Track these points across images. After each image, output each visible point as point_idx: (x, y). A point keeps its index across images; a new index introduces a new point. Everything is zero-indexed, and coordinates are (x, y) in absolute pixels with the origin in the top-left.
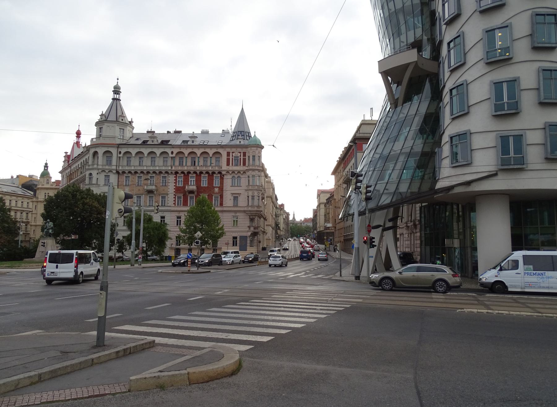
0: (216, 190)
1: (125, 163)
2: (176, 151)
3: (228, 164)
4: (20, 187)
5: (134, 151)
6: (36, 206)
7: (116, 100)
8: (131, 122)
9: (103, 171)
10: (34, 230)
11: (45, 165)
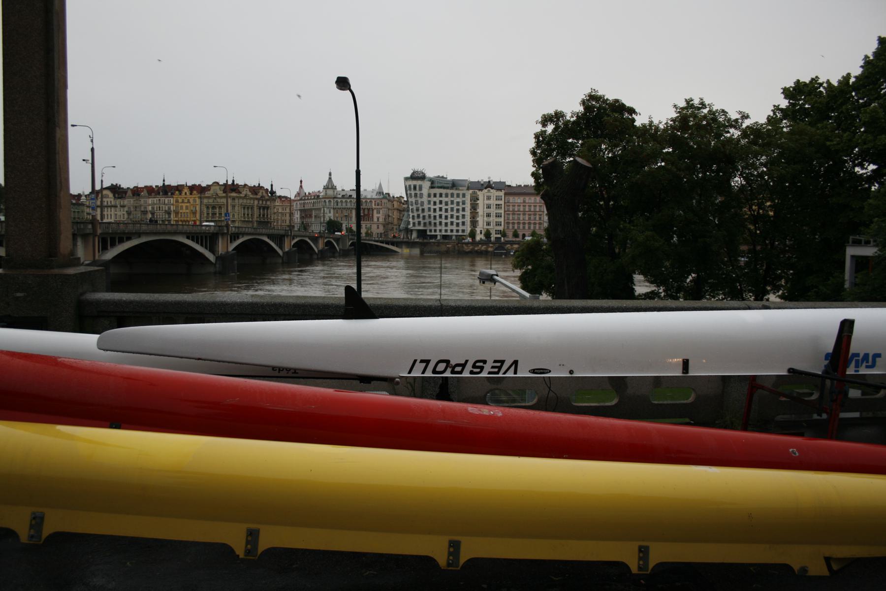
0: (371, 215)
1: (336, 204)
3: (375, 205)
5: (339, 200)
7: (330, 178)
8: (336, 187)
9: (329, 208)
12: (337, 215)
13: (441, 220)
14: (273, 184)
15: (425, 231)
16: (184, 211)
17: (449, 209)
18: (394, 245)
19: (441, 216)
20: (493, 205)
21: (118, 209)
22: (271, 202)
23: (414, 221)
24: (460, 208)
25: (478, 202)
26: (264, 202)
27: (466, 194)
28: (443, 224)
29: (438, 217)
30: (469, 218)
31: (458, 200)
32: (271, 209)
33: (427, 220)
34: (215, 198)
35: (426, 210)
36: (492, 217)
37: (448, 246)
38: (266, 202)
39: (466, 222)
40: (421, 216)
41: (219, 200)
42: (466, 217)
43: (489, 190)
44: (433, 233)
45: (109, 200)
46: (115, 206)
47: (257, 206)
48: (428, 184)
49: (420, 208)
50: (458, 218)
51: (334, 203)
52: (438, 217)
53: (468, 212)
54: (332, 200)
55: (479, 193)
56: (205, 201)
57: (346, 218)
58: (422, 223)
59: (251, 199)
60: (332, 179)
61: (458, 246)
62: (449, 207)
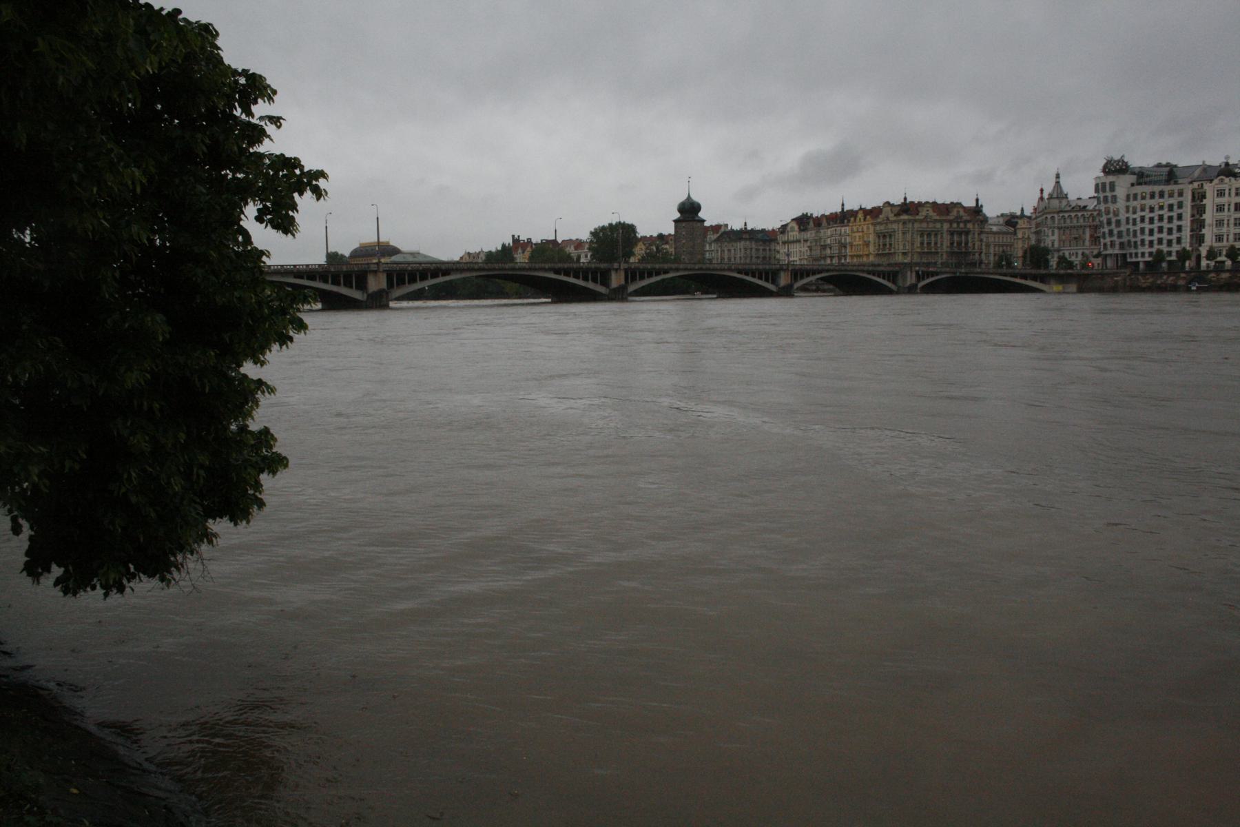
1: (1062, 221)
2: (1089, 213)
5: (1066, 215)
7: (1058, 183)
8: (1066, 195)
9: (1051, 228)
12: (1064, 237)
13: (1143, 237)
15: (1124, 256)
16: (857, 243)
17: (1156, 218)
18: (1036, 281)
19: (1142, 230)
20: (1229, 205)
21: (802, 245)
22: (974, 224)
23: (1106, 241)
24: (1174, 214)
25: (1205, 201)
26: (962, 225)
27: (1185, 191)
28: (1147, 243)
29: (1139, 232)
30: (1189, 229)
31: (1172, 201)
32: (974, 234)
33: (1125, 239)
34: (886, 223)
35: (1123, 221)
36: (1225, 226)
37: (1116, 279)
38: (965, 225)
39: (1184, 237)
40: (1115, 232)
41: (890, 226)
42: (1183, 229)
43: (1222, 179)
44: (1134, 260)
45: (794, 233)
46: (799, 241)
47: (947, 231)
48: (1133, 179)
49: (1114, 220)
50: (1170, 231)
51: (1059, 220)
52: (1139, 232)
53: (1187, 220)
54: (1056, 216)
55: (1208, 187)
56: (878, 228)
57: (1077, 241)
58: (1117, 243)
59: (936, 221)
60: (1061, 183)
61: (1131, 279)
62: (1155, 215)
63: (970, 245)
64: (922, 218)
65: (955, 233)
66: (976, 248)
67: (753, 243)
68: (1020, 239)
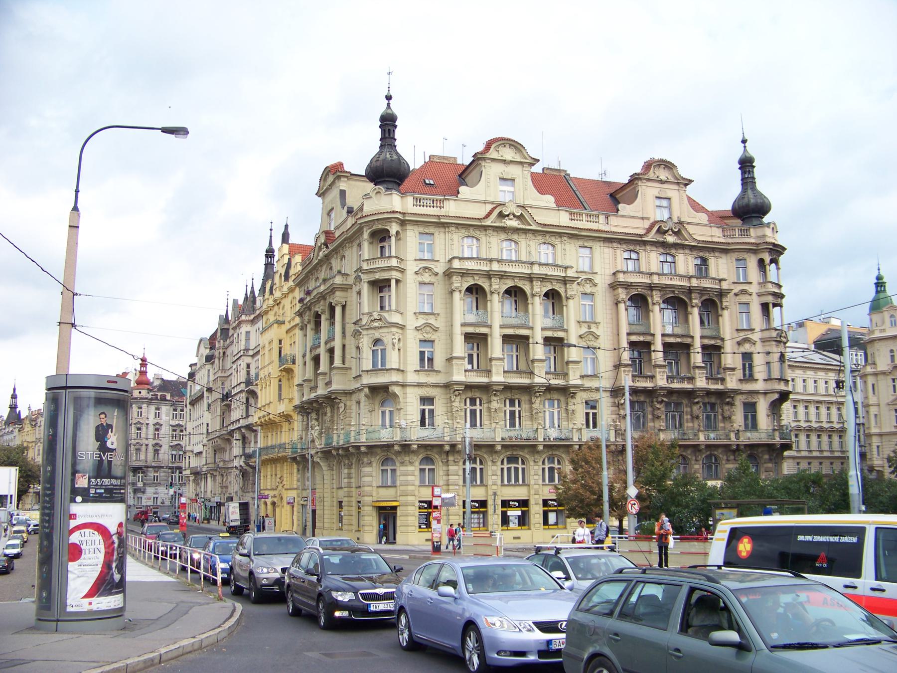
4: (812, 347)
6: (873, 385)
10: (878, 447)
11: (876, 281)
14: (752, 152)
47: (614, 286)
59: (549, 233)
63: (731, 358)
64: (479, 211)
65: (657, 296)
66: (760, 372)
67: (165, 409)
68: (884, 373)
